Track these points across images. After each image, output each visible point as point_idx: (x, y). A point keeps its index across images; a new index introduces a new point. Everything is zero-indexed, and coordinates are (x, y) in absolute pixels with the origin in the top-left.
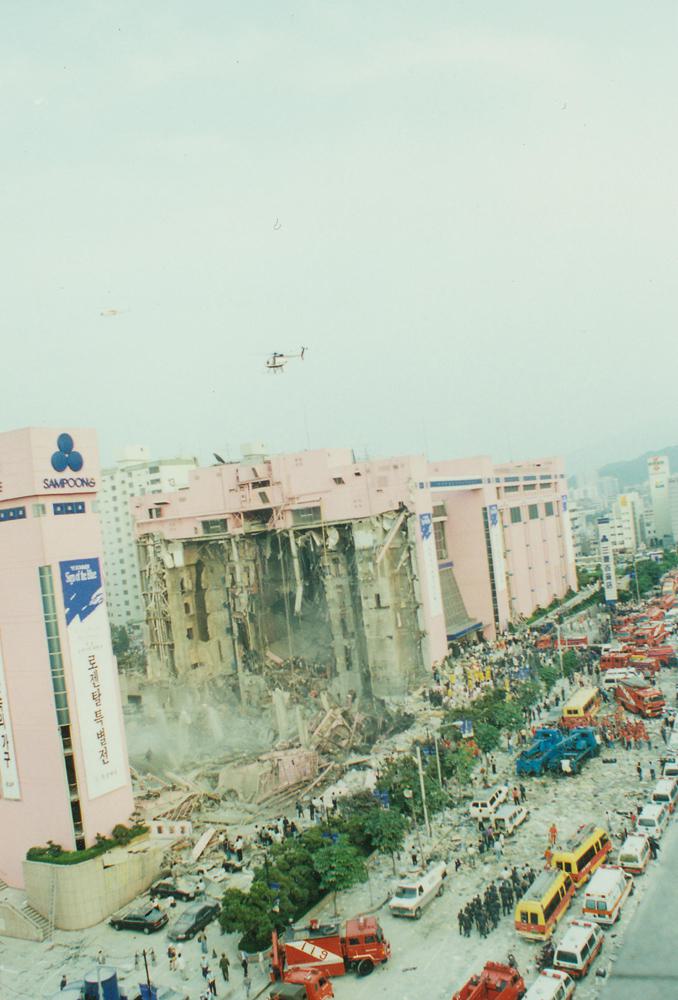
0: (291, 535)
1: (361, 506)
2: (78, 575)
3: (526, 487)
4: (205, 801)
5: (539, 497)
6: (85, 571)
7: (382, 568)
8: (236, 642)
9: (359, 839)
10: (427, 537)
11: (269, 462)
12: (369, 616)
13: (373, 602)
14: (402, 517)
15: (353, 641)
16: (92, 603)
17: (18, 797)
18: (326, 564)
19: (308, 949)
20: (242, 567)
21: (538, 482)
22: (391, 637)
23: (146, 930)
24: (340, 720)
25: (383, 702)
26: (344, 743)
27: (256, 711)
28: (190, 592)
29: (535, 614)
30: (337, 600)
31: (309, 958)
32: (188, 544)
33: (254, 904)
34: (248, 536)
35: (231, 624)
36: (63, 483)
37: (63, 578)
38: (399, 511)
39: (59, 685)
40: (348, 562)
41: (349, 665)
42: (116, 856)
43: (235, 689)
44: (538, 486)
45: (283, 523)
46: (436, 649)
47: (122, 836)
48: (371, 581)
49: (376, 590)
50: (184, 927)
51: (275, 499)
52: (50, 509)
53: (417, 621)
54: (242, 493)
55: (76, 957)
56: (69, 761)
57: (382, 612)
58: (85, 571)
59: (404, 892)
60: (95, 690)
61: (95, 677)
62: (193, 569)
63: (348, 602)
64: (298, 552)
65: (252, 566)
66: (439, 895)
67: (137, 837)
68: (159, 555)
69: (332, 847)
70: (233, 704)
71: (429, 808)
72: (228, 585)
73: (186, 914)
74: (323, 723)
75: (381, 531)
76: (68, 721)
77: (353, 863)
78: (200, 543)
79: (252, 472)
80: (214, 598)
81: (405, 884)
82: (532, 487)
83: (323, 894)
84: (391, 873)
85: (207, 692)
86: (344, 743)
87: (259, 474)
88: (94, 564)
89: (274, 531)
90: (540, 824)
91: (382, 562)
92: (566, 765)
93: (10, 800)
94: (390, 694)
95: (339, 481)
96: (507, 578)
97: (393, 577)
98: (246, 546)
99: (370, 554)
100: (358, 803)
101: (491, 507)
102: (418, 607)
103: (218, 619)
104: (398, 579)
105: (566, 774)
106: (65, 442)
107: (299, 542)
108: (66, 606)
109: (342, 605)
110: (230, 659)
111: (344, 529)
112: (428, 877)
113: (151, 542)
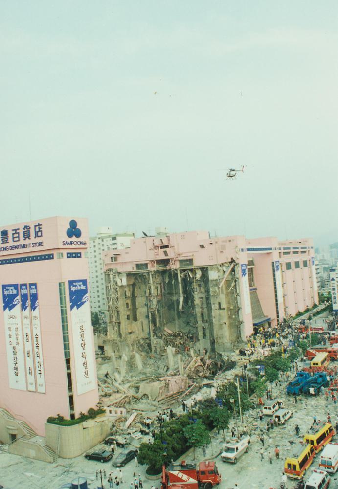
0: (178, 272)
1: (212, 259)
2: (77, 287)
3: (294, 253)
4: (133, 399)
5: (301, 258)
6: (80, 285)
7: (222, 289)
8: (150, 322)
9: (207, 422)
10: (244, 275)
11: (169, 237)
12: (215, 312)
13: (217, 306)
14: (232, 265)
15: (207, 324)
16: (83, 301)
17: (44, 392)
18: (195, 287)
19: (180, 475)
20: (154, 287)
21: (300, 250)
22: (225, 323)
23: (102, 461)
24: (199, 363)
25: (220, 355)
26: (201, 374)
27: (159, 357)
28: (129, 297)
29: (297, 315)
30: (200, 304)
31: (180, 480)
32: (129, 275)
33: (155, 451)
34: (158, 272)
35: (148, 313)
36: (71, 243)
37: (70, 288)
38: (231, 262)
39: (66, 339)
40: (206, 286)
41: (204, 335)
42: (89, 423)
43: (149, 345)
44: (300, 253)
45: (174, 266)
46: (248, 330)
47: (92, 414)
48: (216, 296)
49: (218, 300)
50: (120, 460)
51: (171, 254)
52: (65, 255)
53: (238, 315)
54: (155, 251)
55: (68, 471)
56: (69, 376)
57: (221, 311)
58: (80, 285)
59: (228, 450)
60: (82, 342)
61: (82, 336)
62: (131, 287)
63: (205, 306)
64: (182, 280)
65: (159, 286)
66: (246, 452)
67: (100, 415)
68: (115, 279)
69: (194, 425)
70: (148, 352)
71: (242, 408)
72: (147, 295)
73: (121, 453)
74: (191, 363)
75: (222, 272)
76: (70, 357)
77: (204, 434)
78: (134, 275)
79: (160, 241)
80: (140, 301)
81: (229, 446)
82: (297, 252)
83: (188, 448)
84: (222, 440)
85: (136, 346)
86: (201, 374)
87: (163, 241)
88: (84, 282)
89: (170, 270)
90: (298, 420)
91: (222, 287)
92: (312, 390)
93: (40, 393)
94: (224, 351)
95: (202, 247)
96: (284, 297)
97: (227, 294)
98: (157, 277)
99: (216, 283)
100: (207, 404)
101: (276, 262)
102: (239, 309)
103: (142, 311)
104: (230, 295)
105: (312, 395)
106: (73, 224)
107: (182, 276)
108: (71, 301)
109: (202, 307)
110: (147, 330)
111: (204, 270)
112: (241, 443)
113: (112, 273)
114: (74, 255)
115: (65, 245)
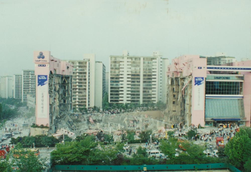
6: (43, 77)
16: (44, 83)
37: (38, 78)
58: (43, 77)
115: (36, 61)
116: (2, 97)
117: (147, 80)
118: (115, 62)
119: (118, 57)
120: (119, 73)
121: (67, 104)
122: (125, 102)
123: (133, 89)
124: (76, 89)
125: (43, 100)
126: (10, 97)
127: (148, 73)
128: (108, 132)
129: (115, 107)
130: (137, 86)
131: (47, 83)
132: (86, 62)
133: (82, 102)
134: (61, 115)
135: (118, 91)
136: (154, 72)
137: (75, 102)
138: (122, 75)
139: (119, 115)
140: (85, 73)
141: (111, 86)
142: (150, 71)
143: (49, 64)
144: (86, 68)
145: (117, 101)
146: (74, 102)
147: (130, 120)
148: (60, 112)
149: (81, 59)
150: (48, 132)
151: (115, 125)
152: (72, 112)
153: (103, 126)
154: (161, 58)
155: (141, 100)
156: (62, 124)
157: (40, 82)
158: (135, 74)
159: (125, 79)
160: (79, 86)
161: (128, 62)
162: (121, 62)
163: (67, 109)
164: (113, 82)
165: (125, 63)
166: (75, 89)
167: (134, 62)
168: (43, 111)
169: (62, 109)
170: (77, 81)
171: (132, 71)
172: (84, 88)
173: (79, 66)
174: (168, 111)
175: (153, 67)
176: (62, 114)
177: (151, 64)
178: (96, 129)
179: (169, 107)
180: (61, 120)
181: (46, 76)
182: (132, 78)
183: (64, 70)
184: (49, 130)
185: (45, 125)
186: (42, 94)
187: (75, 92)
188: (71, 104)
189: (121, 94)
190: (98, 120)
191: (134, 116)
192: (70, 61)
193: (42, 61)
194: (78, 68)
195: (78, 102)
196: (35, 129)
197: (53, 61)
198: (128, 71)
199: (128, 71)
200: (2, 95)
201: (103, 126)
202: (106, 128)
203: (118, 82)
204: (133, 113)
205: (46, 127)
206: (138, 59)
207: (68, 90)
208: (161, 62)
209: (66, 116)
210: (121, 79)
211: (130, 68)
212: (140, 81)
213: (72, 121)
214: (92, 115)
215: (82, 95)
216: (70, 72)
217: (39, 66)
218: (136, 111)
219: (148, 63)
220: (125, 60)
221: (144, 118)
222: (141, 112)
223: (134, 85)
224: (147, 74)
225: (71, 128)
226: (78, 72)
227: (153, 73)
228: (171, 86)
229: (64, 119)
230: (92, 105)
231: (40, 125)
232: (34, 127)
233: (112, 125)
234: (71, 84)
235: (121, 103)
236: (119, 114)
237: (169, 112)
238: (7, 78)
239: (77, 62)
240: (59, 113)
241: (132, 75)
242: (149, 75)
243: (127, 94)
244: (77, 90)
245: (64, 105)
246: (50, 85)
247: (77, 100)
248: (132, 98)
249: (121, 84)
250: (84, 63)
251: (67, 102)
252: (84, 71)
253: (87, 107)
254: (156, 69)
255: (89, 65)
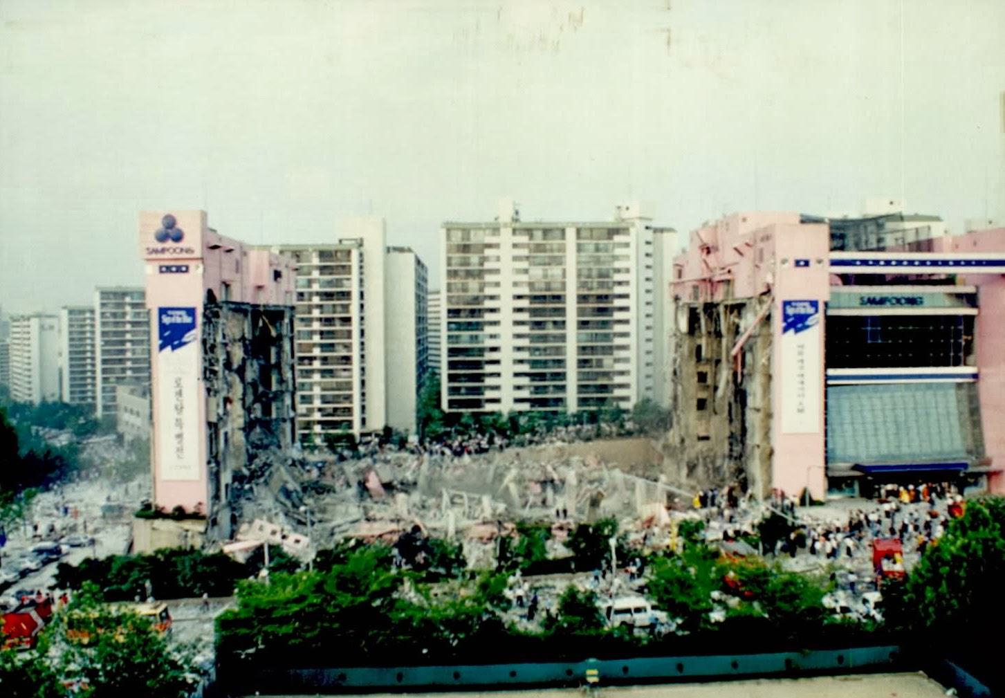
16: (185, 339)
36: (163, 250)
37: (160, 319)
58: (180, 316)
60: (179, 403)
67: (194, 521)
106: (170, 223)
108: (161, 337)
114: (174, 269)
116: (18, 400)
117: (594, 316)
118: (465, 248)
119: (478, 227)
120: (481, 290)
121: (276, 420)
122: (506, 407)
123: (540, 355)
124: (311, 359)
125: (182, 408)
126: (50, 400)
127: (598, 288)
128: (442, 528)
129: (467, 426)
130: (555, 341)
131: (194, 339)
132: (349, 252)
133: (335, 409)
134: (253, 467)
135: (478, 365)
136: (620, 283)
137: (310, 411)
138: (492, 298)
139: (485, 459)
140: (347, 295)
141: (449, 343)
142: (603, 282)
143: (203, 263)
144: (350, 273)
145: (478, 404)
146: (304, 411)
147: (531, 480)
148: (247, 451)
149: (329, 240)
150: (205, 537)
151: (471, 499)
152: (299, 451)
153: (424, 507)
154: (647, 228)
155: (572, 397)
156: (260, 501)
157: (168, 336)
158: (543, 293)
159: (506, 316)
160: (322, 346)
161: (515, 246)
162: (489, 246)
163: (279, 441)
164: (460, 326)
165: (506, 252)
166: (306, 362)
167: (539, 248)
168: (182, 450)
169: (259, 443)
170: (316, 326)
171: (532, 281)
172: (344, 353)
173: (323, 269)
174: (677, 440)
175: (617, 265)
176: (257, 461)
177: (606, 251)
178: (392, 521)
179: (682, 423)
180: (254, 486)
181: (191, 312)
182: (534, 312)
183: (260, 284)
184: (207, 529)
185: (190, 509)
186: (178, 383)
187: (309, 373)
188: (292, 420)
189: (492, 375)
190: (402, 484)
191: (543, 464)
192: (284, 248)
193: (175, 250)
194: (316, 274)
195: (320, 410)
196: (152, 524)
197: (217, 251)
198: (515, 284)
199: (515, 284)
200: (16, 390)
201: (424, 507)
202: (435, 515)
203: (478, 326)
204: (540, 451)
205: (196, 516)
206: (558, 233)
207: (278, 366)
208: (648, 243)
209: (272, 469)
210: (488, 317)
211: (526, 271)
212: (564, 322)
213: (299, 489)
214: (375, 461)
215: (337, 383)
216: (287, 292)
217: (161, 272)
218: (552, 442)
219: (597, 249)
220: (506, 238)
221: (584, 468)
222: (573, 445)
223: (544, 338)
224: (593, 292)
225: (296, 516)
226: (318, 294)
227: (618, 290)
228: (687, 337)
229: (266, 483)
230: (377, 423)
231: (169, 509)
232: (148, 517)
233: (457, 500)
234: (292, 339)
235: (492, 413)
236: (483, 455)
237: (683, 441)
238: (34, 323)
239: (315, 250)
240: (244, 459)
241: (535, 298)
242: (600, 298)
243: (517, 375)
244: (317, 365)
245: (267, 424)
246: (208, 346)
247: (317, 403)
248: (537, 389)
249: (492, 336)
250: (339, 254)
251: (278, 414)
252: (342, 286)
253: (356, 430)
254: (627, 271)
255: (361, 261)
